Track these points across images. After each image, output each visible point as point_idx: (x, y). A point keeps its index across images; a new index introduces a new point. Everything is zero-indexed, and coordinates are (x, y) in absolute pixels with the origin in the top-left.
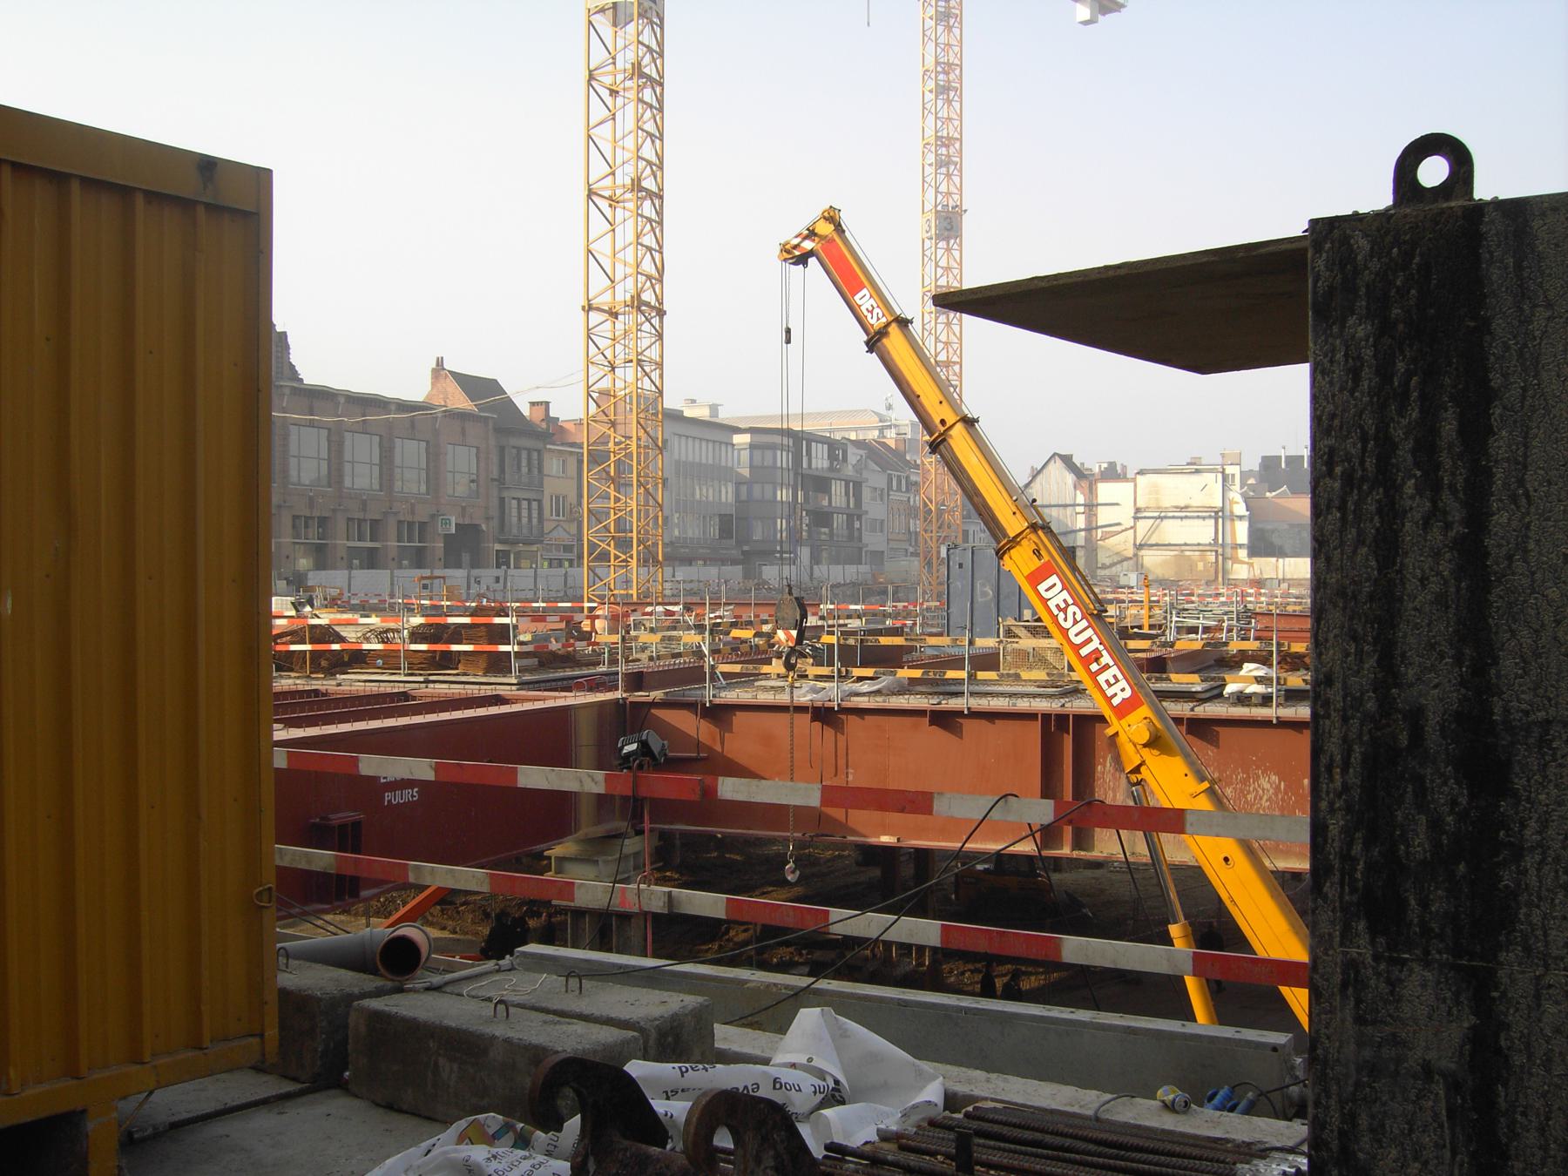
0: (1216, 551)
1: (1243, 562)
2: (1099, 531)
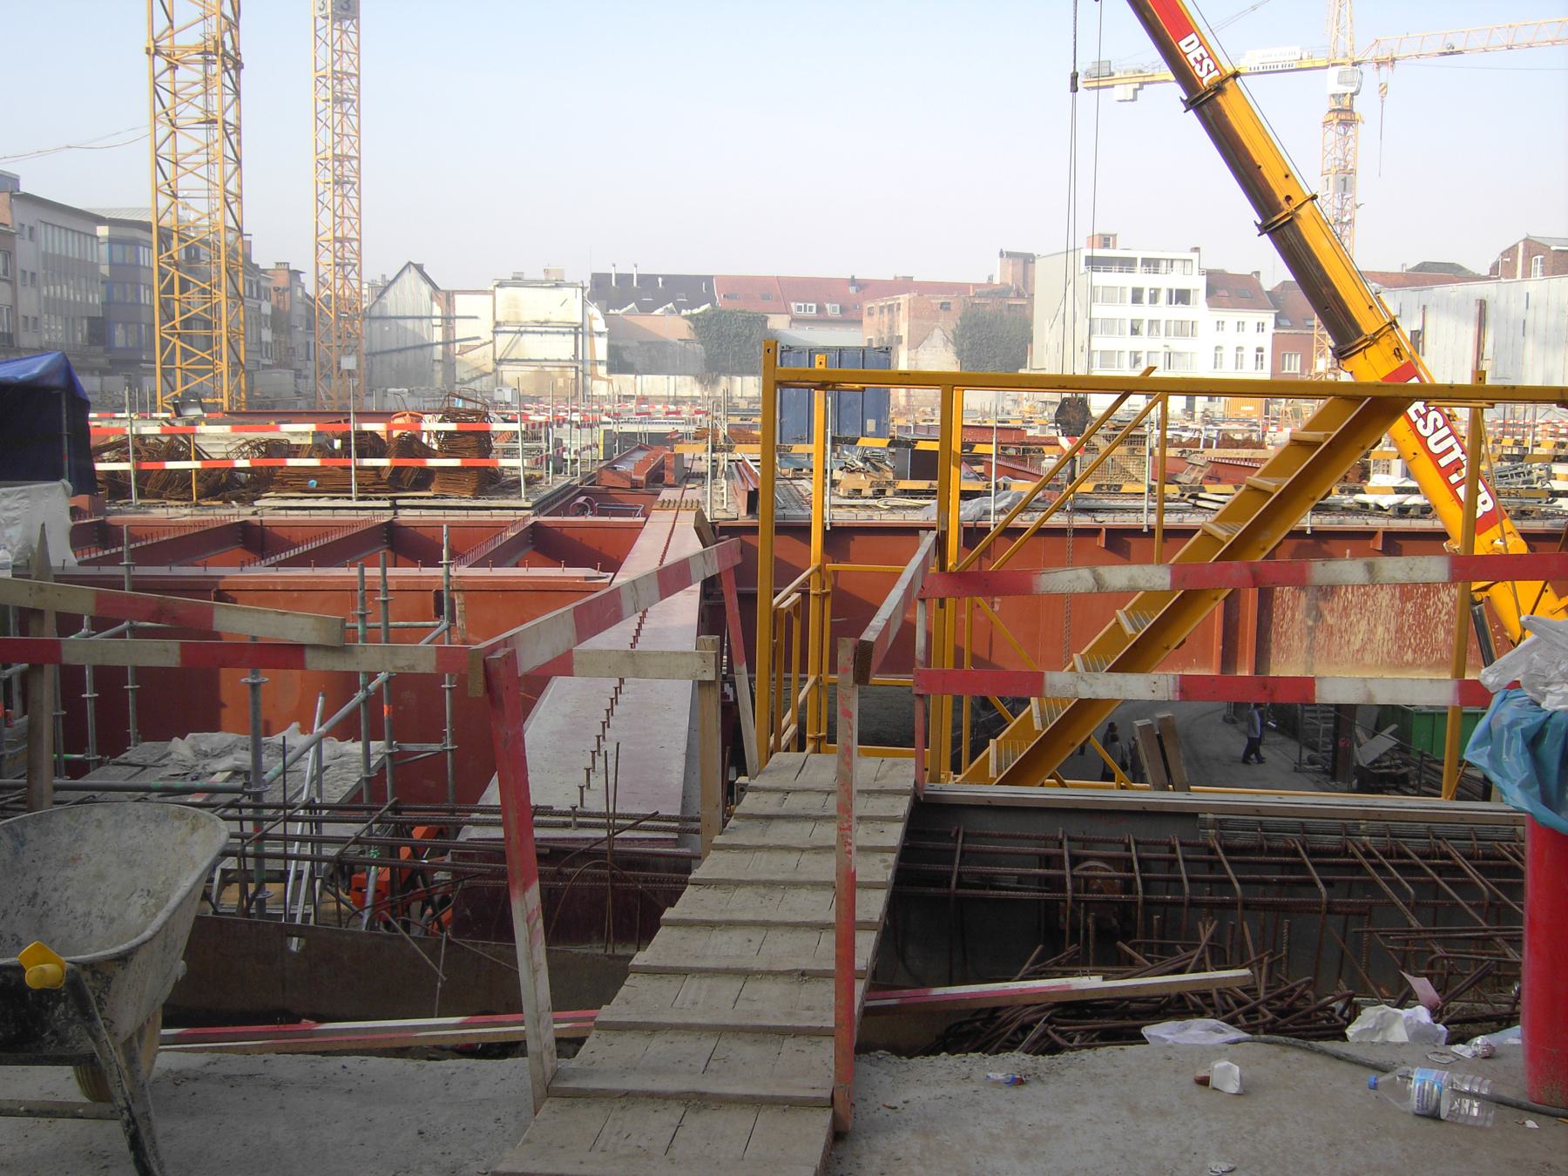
0: (577, 368)
1: (601, 379)
2: (457, 345)
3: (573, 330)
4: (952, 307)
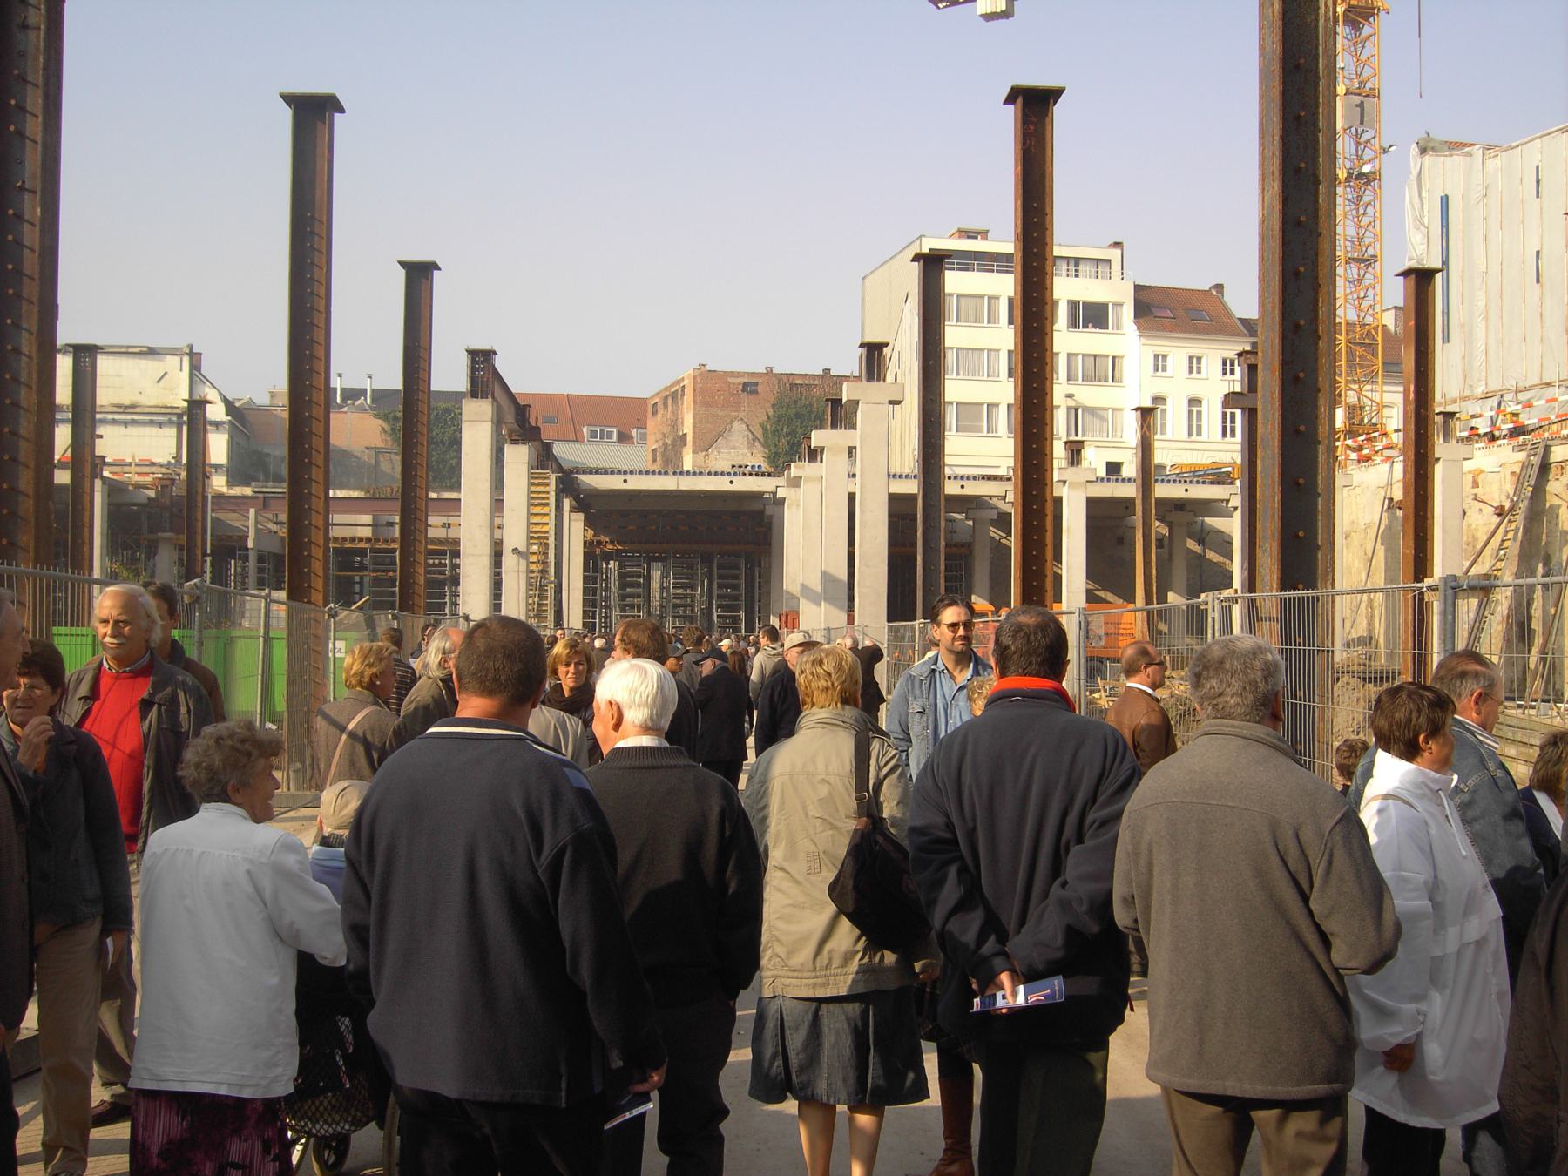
3: (174, 418)
4: (760, 388)
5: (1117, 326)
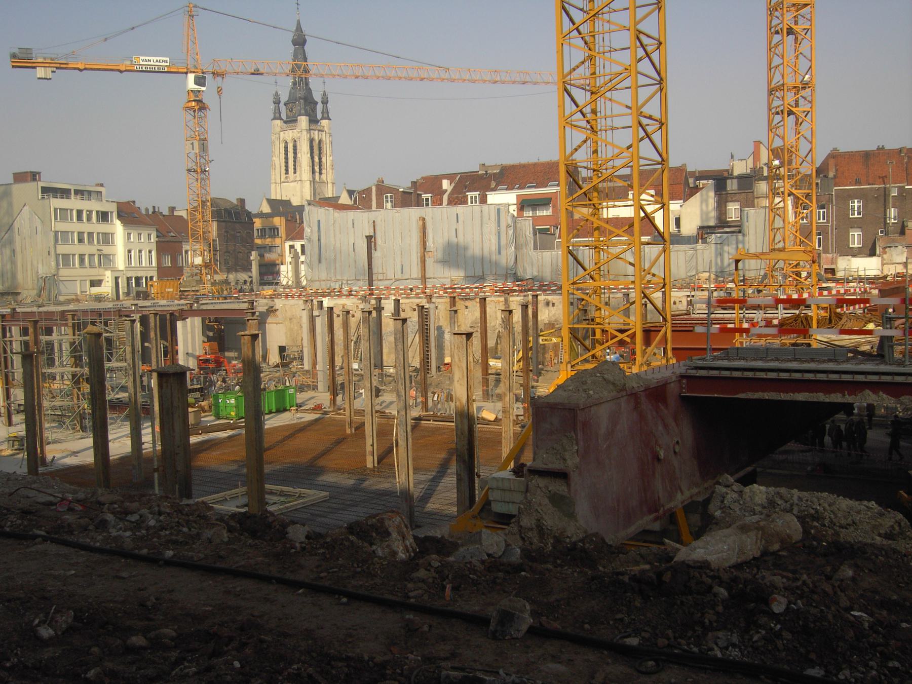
5: (112, 221)
